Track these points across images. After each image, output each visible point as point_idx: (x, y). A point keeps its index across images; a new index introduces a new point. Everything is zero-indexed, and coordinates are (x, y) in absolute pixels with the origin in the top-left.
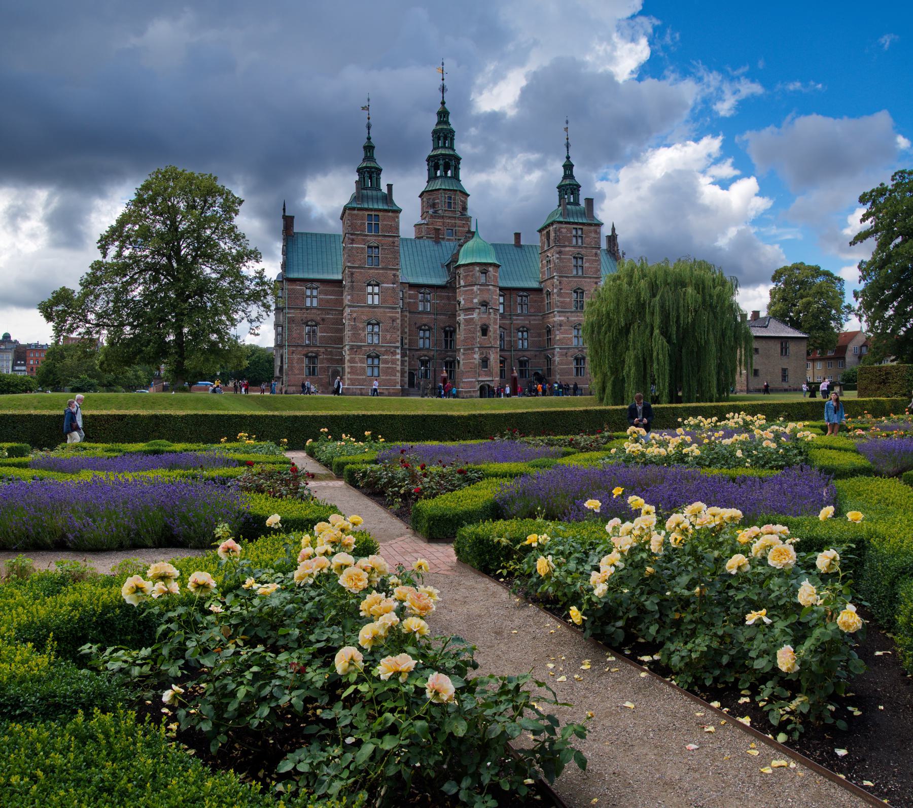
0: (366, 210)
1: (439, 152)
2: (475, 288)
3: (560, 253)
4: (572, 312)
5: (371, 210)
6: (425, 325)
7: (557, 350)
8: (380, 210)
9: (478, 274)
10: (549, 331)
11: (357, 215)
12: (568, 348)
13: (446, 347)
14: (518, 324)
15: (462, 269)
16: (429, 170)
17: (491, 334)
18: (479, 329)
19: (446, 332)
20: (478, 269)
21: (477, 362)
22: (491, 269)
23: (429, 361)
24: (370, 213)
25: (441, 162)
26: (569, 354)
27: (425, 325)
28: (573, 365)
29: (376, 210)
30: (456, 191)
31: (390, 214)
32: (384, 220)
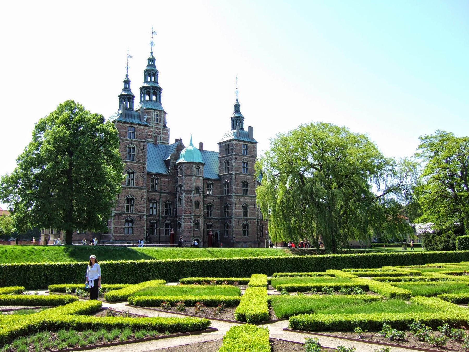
0: (128, 123)
1: (151, 84)
2: (193, 178)
3: (236, 159)
4: (241, 196)
5: (132, 123)
6: (154, 200)
7: (233, 219)
8: (137, 124)
9: (194, 169)
10: (227, 208)
11: (122, 126)
12: (240, 219)
13: (166, 214)
14: (207, 201)
15: (184, 166)
16: (141, 95)
17: (200, 207)
18: (194, 204)
19: (166, 205)
20: (194, 166)
21: (192, 224)
22: (201, 167)
23: (156, 223)
24: (130, 125)
25: (152, 91)
26: (240, 222)
27: (154, 200)
28: (242, 229)
29: (134, 124)
30: (162, 111)
31: (143, 127)
32: (138, 131)
